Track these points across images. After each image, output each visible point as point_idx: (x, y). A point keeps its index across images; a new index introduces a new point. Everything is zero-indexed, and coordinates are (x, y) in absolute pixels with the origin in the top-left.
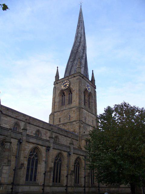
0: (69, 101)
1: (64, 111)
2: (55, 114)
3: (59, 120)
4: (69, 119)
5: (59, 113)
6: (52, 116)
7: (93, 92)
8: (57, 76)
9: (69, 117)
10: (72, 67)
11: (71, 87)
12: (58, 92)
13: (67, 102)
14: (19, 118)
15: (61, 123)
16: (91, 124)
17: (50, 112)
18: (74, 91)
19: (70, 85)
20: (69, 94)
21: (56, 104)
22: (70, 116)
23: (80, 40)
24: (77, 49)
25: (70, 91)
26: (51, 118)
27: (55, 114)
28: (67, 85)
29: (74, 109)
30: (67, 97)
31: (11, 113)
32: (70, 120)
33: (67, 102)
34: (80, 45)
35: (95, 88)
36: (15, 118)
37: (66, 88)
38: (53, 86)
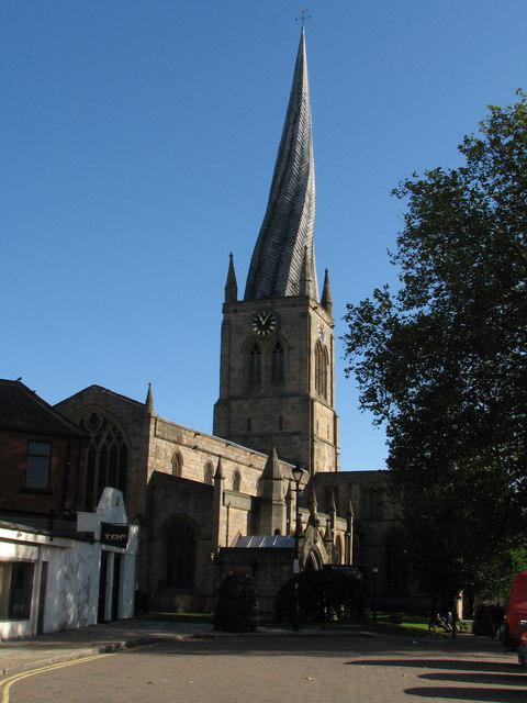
0: (274, 372)
1: (262, 401)
4: (277, 425)
5: (245, 406)
8: (231, 286)
9: (277, 419)
10: (278, 264)
11: (283, 333)
12: (239, 342)
13: (265, 376)
16: (324, 437)
17: (216, 396)
18: (293, 348)
19: (279, 327)
21: (234, 375)
22: (281, 418)
25: (278, 345)
27: (234, 405)
28: (272, 328)
29: (292, 400)
30: (265, 361)
33: (265, 376)
37: (266, 333)
38: (220, 317)
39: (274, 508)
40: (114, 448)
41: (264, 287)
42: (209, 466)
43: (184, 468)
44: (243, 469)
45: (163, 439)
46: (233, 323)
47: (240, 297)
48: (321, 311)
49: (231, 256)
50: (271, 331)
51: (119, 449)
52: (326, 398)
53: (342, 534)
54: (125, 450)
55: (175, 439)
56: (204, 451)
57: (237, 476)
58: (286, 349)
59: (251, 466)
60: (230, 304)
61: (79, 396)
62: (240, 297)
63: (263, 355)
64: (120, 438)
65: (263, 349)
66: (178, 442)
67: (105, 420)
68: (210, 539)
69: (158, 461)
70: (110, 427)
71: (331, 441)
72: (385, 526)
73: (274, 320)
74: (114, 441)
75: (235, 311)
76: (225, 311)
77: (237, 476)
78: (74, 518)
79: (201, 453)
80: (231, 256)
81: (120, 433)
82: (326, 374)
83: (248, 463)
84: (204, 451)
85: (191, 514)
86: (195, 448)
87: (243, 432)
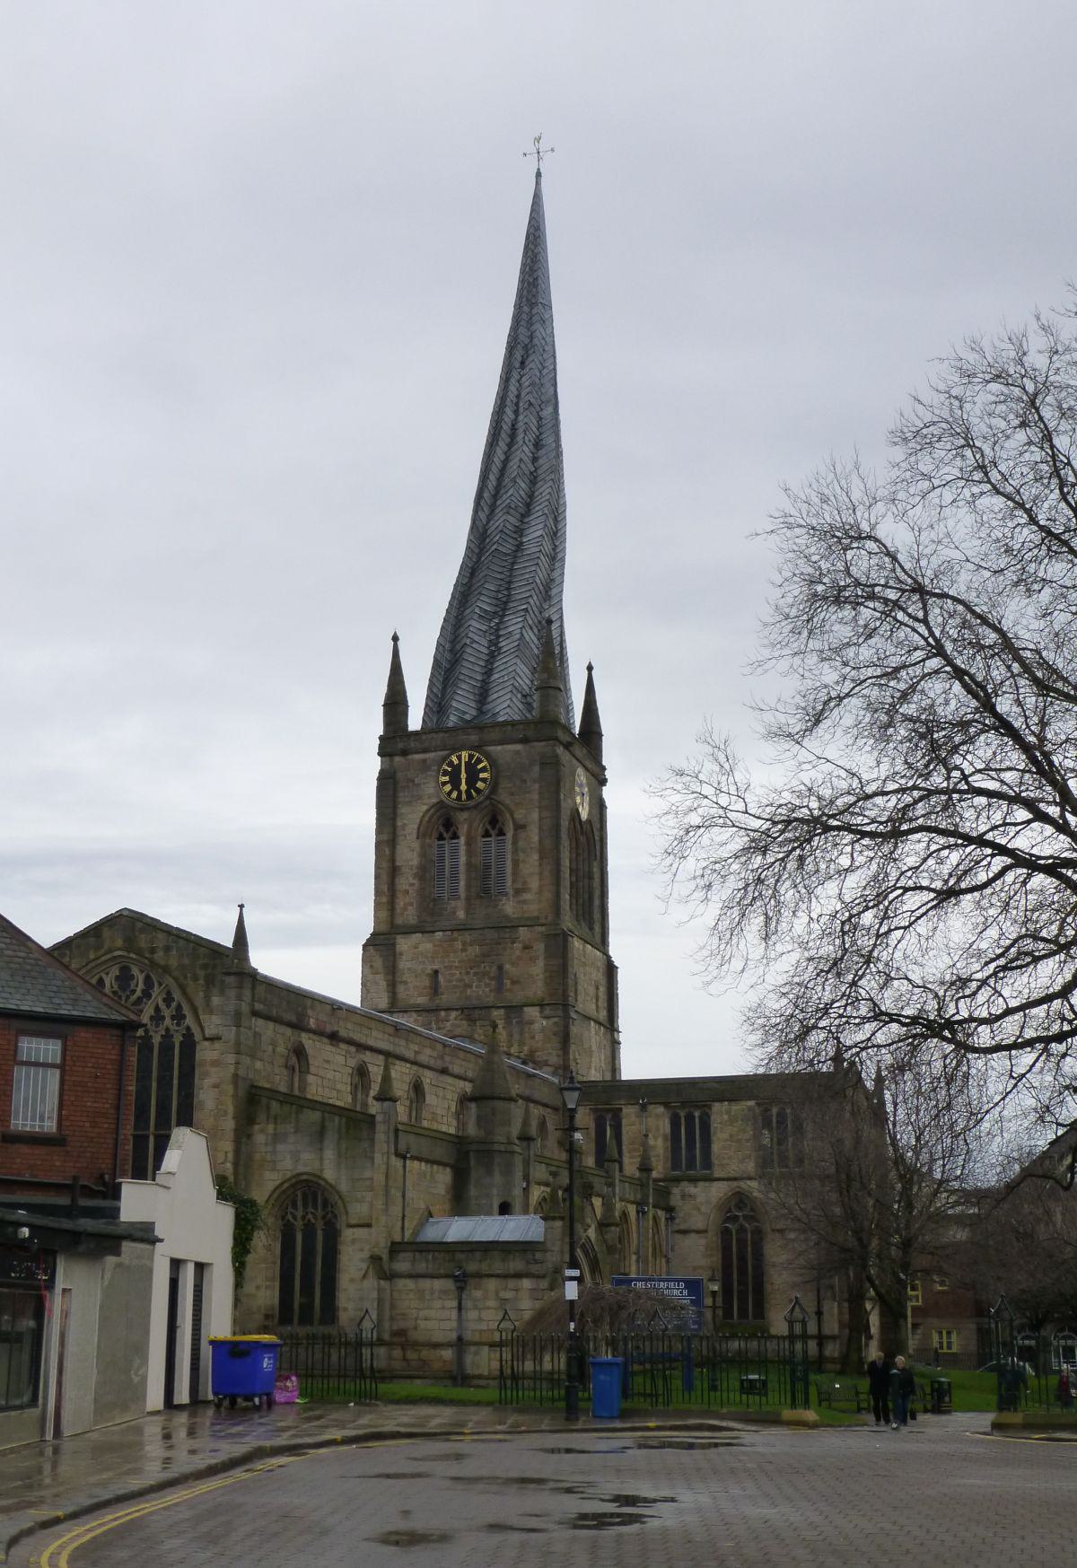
2: (404, 944)
3: (427, 982)
6: (380, 947)
7: (596, 826)
8: (395, 703)
10: (492, 657)
11: (503, 796)
12: (412, 816)
14: (423, 1058)
15: (446, 998)
16: (590, 1008)
17: (366, 925)
19: (494, 785)
20: (487, 834)
22: (500, 968)
23: (535, 460)
24: (520, 531)
25: (494, 821)
26: (378, 963)
27: (404, 944)
28: (480, 785)
31: (403, 1043)
32: (499, 989)
34: (531, 496)
35: (603, 782)
36: (414, 1063)
38: (375, 764)
39: (497, 1160)
40: (168, 1036)
41: (462, 705)
42: (362, 1072)
43: (310, 1079)
44: (428, 1078)
45: (268, 1018)
46: (399, 775)
47: (415, 721)
48: (579, 751)
49: (395, 638)
50: (478, 791)
51: (178, 1039)
52: (591, 929)
53: (632, 1209)
54: (189, 1046)
55: (292, 1018)
56: (350, 1042)
57: (418, 1088)
58: (510, 835)
59: (444, 1071)
60: (395, 740)
61: (95, 931)
62: (415, 721)
63: (462, 840)
64: (179, 1017)
65: (463, 830)
66: (299, 1026)
67: (148, 980)
68: (369, 1226)
69: (258, 1065)
70: (157, 994)
71: (603, 1015)
72: (718, 1191)
73: (484, 770)
74: (168, 1021)
75: (404, 753)
76: (383, 752)
77: (418, 1088)
78: (115, 1193)
79: (343, 1046)
80: (395, 638)
81: (179, 1007)
82: (591, 878)
83: (439, 1064)
84: (350, 1042)
85: (329, 1174)
86: (334, 1038)
87: (421, 1000)
